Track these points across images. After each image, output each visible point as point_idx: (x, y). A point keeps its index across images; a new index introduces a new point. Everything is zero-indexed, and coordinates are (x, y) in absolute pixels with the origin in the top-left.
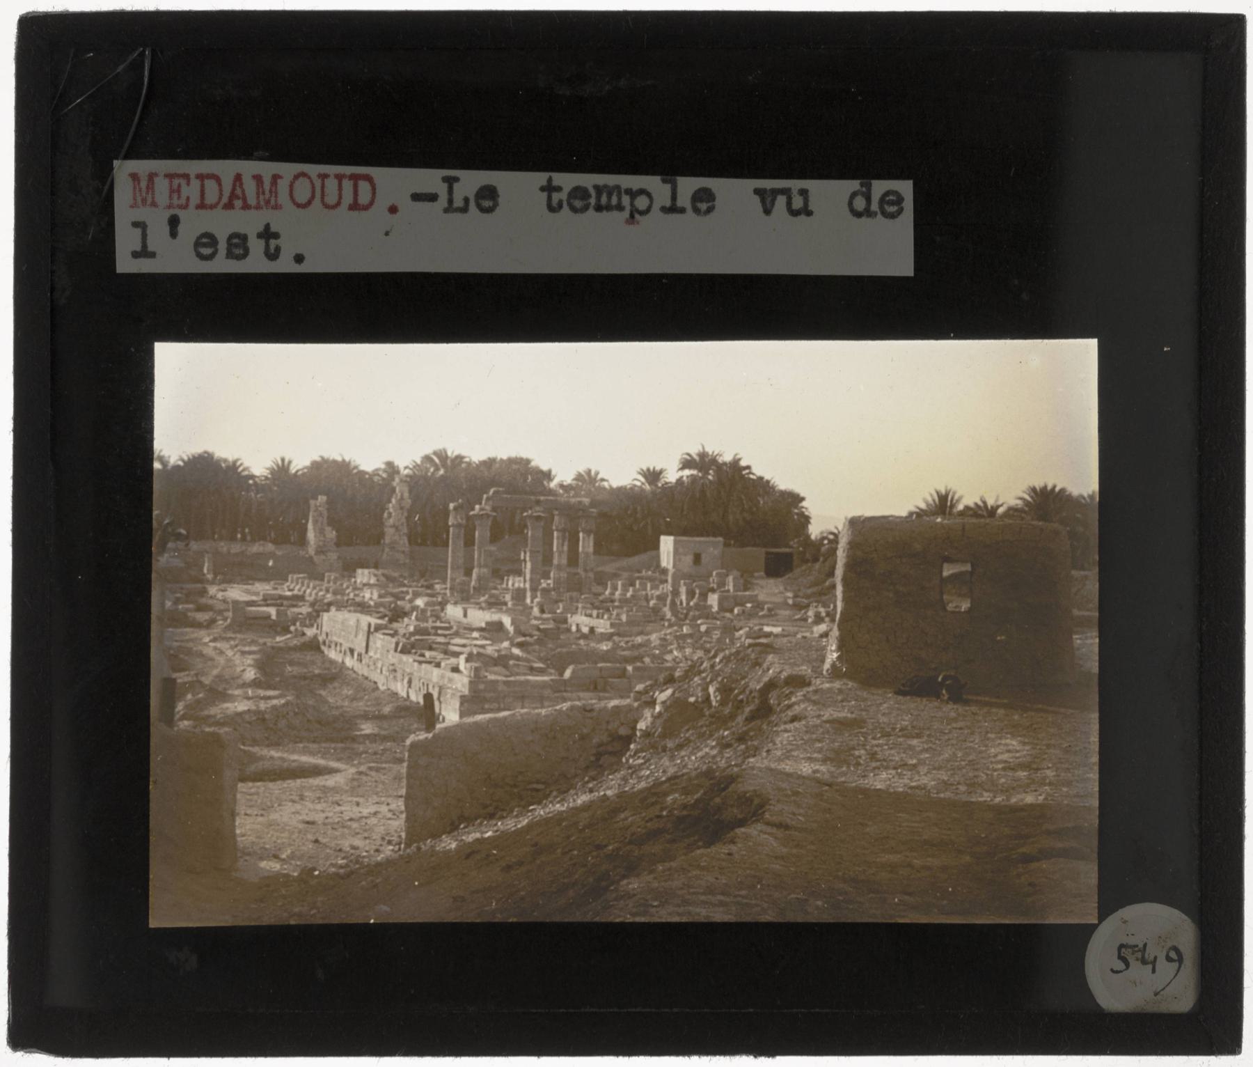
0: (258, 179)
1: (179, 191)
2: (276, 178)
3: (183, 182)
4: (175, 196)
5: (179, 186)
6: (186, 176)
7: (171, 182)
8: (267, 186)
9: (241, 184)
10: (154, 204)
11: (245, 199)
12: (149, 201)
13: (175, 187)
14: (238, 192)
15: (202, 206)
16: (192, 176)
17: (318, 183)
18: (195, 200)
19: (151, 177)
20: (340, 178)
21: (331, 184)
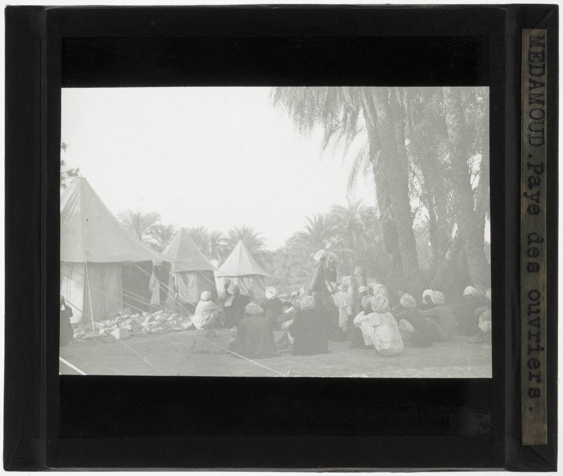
0: (542, 95)
1: (537, 56)
2: (542, 103)
3: (541, 58)
4: (535, 55)
5: (539, 57)
6: (543, 60)
7: (540, 53)
8: (541, 98)
9: (540, 86)
10: (531, 46)
11: (533, 88)
12: (533, 44)
13: (540, 55)
14: (538, 85)
15: (531, 67)
16: (543, 63)
17: (539, 121)
18: (533, 65)
19: (544, 45)
20: (543, 131)
21: (539, 127)
